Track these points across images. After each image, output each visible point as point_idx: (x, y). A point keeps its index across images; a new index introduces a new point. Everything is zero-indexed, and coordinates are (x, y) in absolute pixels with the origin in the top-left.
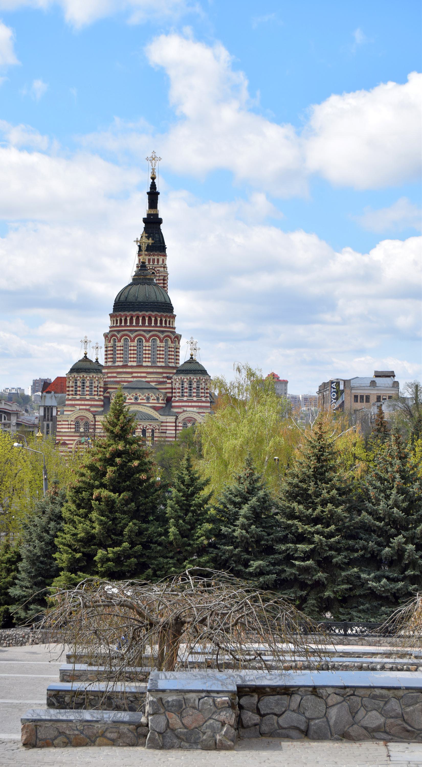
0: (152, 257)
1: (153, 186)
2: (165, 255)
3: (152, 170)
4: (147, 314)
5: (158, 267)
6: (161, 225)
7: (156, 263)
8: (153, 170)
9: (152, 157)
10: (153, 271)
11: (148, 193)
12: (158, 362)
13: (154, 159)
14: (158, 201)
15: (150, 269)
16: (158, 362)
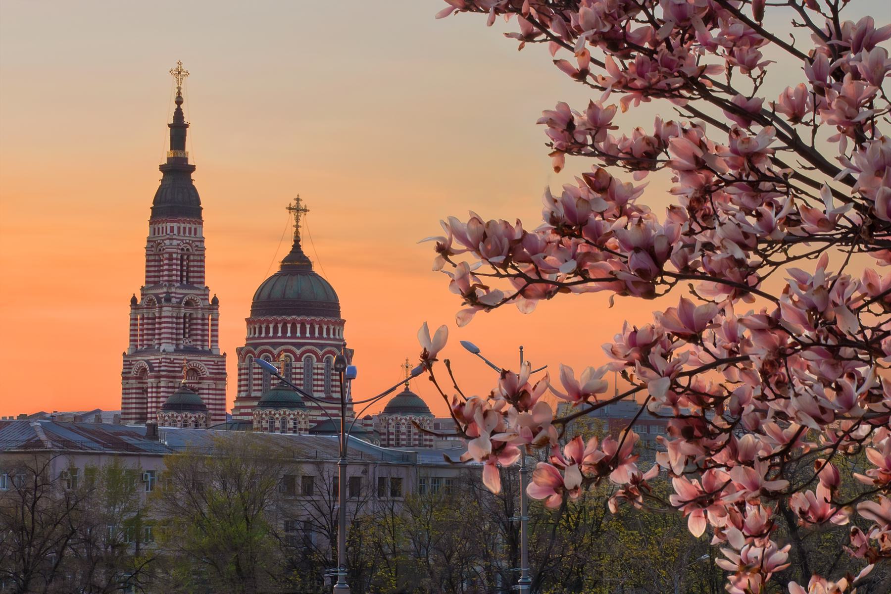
0: (188, 226)
1: (179, 114)
2: (201, 223)
3: (177, 90)
4: (318, 319)
5: (198, 241)
6: (193, 176)
7: (193, 235)
8: (179, 88)
9: (177, 70)
10: (189, 247)
11: (169, 125)
12: (333, 392)
13: (179, 73)
14: (187, 138)
15: (186, 243)
16: (333, 392)
